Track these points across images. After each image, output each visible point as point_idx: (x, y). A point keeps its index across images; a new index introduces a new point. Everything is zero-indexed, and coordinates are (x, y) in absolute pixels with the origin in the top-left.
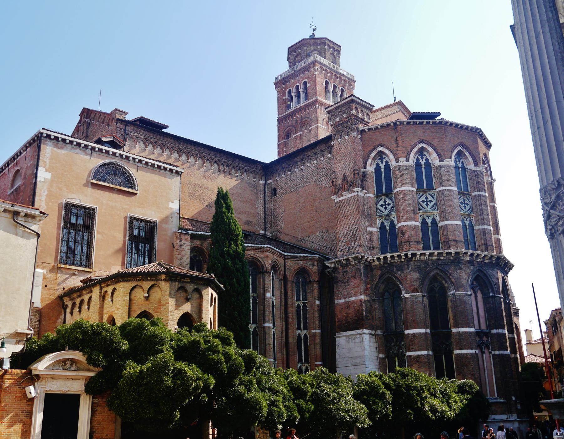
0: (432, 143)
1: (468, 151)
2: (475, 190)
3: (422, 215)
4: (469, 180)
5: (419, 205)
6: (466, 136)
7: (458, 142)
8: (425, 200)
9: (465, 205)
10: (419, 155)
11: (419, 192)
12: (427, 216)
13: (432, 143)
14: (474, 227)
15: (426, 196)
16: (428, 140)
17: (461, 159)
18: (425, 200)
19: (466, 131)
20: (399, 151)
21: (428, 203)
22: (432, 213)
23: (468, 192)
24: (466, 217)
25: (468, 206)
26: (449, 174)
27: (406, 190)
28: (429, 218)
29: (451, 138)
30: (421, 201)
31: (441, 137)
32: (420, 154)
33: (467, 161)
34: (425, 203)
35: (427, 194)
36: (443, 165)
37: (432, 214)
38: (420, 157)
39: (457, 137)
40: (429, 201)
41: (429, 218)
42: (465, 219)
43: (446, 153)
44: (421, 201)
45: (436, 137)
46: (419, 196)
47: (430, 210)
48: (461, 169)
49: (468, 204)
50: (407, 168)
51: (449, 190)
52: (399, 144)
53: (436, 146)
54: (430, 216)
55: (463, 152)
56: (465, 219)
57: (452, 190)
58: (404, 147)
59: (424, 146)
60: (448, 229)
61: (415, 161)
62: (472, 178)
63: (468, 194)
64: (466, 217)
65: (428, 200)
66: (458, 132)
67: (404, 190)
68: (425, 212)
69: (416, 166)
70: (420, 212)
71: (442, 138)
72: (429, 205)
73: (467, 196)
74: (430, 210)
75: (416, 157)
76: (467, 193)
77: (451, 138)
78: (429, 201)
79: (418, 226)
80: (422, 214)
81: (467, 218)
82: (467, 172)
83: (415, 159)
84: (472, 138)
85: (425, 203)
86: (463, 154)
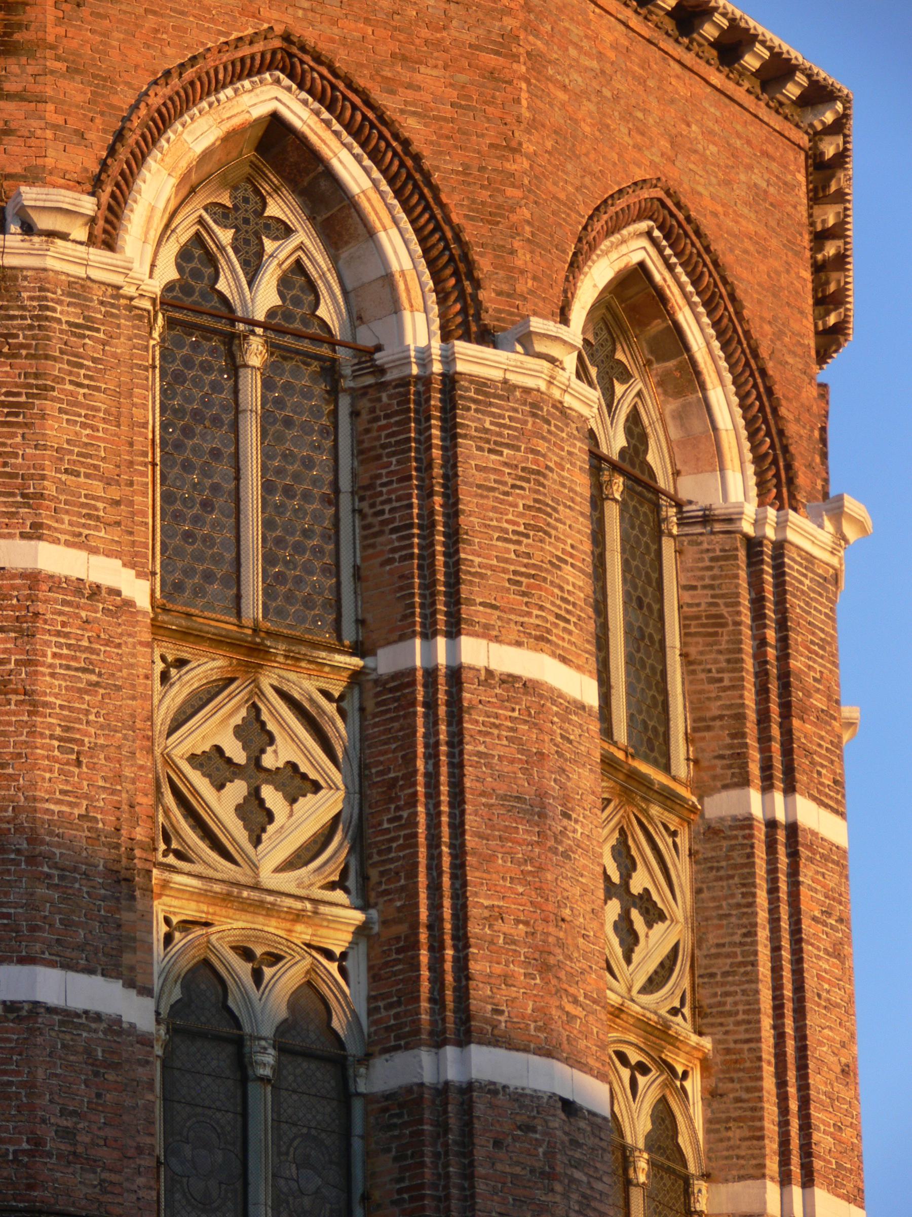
0: (380, 97)
1: (710, 305)
2: (740, 758)
3: (187, 925)
4: (686, 634)
5: (169, 799)
6: (709, 134)
7: (639, 174)
8: (236, 752)
9: (625, 916)
10: (222, 214)
11: (185, 635)
12: (246, 954)
13: (390, 103)
14: (700, 1185)
15: (258, 711)
16: (343, 60)
17: (625, 376)
18: (236, 752)
19: (717, 79)
20: (19, 97)
21: (271, 796)
22: (298, 917)
23: (667, 769)
24: (634, 1057)
25: (659, 927)
26: (538, 507)
27: (56, 583)
28: (257, 976)
29: (579, 96)
30: (193, 759)
31: (492, 60)
32: (225, 199)
33: (681, 416)
34: (237, 790)
35: (266, 681)
36: (482, 385)
37: (303, 933)
38: (226, 236)
39: (628, 115)
40: (272, 776)
41: (257, 976)
42: (625, 1073)
43: (523, 258)
44: (193, 759)
45: (437, 45)
46: (178, 694)
47: (287, 881)
48: (618, 487)
49: (654, 915)
50: (89, 325)
51: (529, 687)
52: (31, 14)
53: (418, 146)
54: (275, 959)
55: (662, 298)
56: (625, 1073)
57: (555, 696)
58: (73, 71)
59: (298, 124)
60: (482, 1149)
61: (168, 272)
62: (718, 621)
63: (669, 799)
64: (634, 1057)
65: (269, 760)
66: (645, 64)
67: (33, 578)
68: (226, 899)
69: (171, 323)
70: (178, 878)
71: (492, 75)
72: (270, 816)
73: (655, 810)
74: (287, 881)
75: (184, 232)
76: (658, 776)
77: (579, 96)
78: (272, 776)
79: (146, 1041)
80: (190, 910)
81: (643, 1069)
82: (668, 547)
83: (171, 250)
84: (756, 178)
85: (237, 790)
86: (657, 326)
